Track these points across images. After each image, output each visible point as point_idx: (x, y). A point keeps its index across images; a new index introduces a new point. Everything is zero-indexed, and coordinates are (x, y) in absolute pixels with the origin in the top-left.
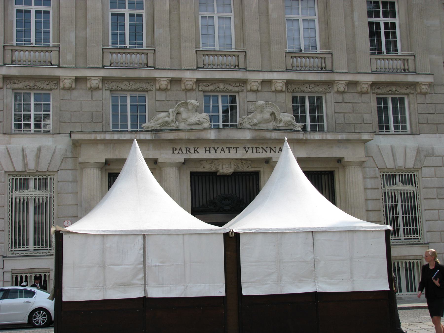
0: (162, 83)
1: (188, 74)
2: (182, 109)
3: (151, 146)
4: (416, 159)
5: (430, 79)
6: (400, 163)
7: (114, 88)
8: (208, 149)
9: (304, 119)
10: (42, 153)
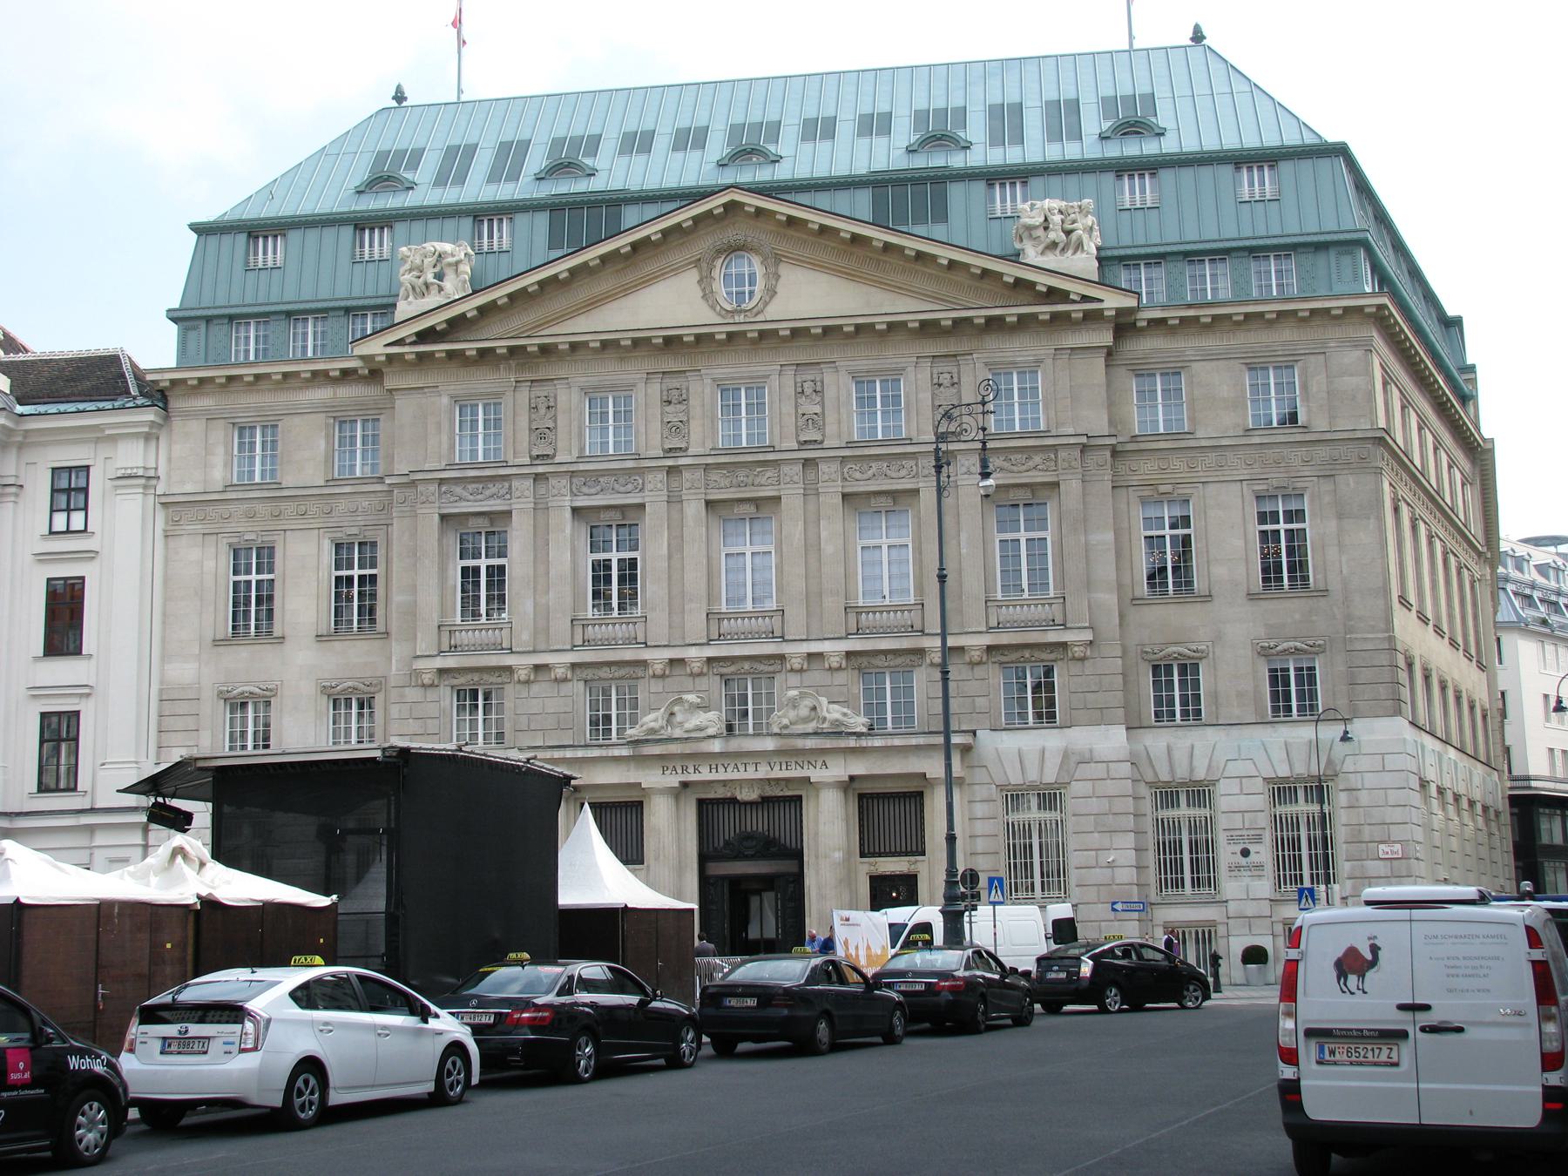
0: (656, 666)
1: (692, 653)
2: (676, 709)
3: (632, 765)
5: (1087, 636)
6: (1033, 776)
7: (589, 678)
8: (714, 766)
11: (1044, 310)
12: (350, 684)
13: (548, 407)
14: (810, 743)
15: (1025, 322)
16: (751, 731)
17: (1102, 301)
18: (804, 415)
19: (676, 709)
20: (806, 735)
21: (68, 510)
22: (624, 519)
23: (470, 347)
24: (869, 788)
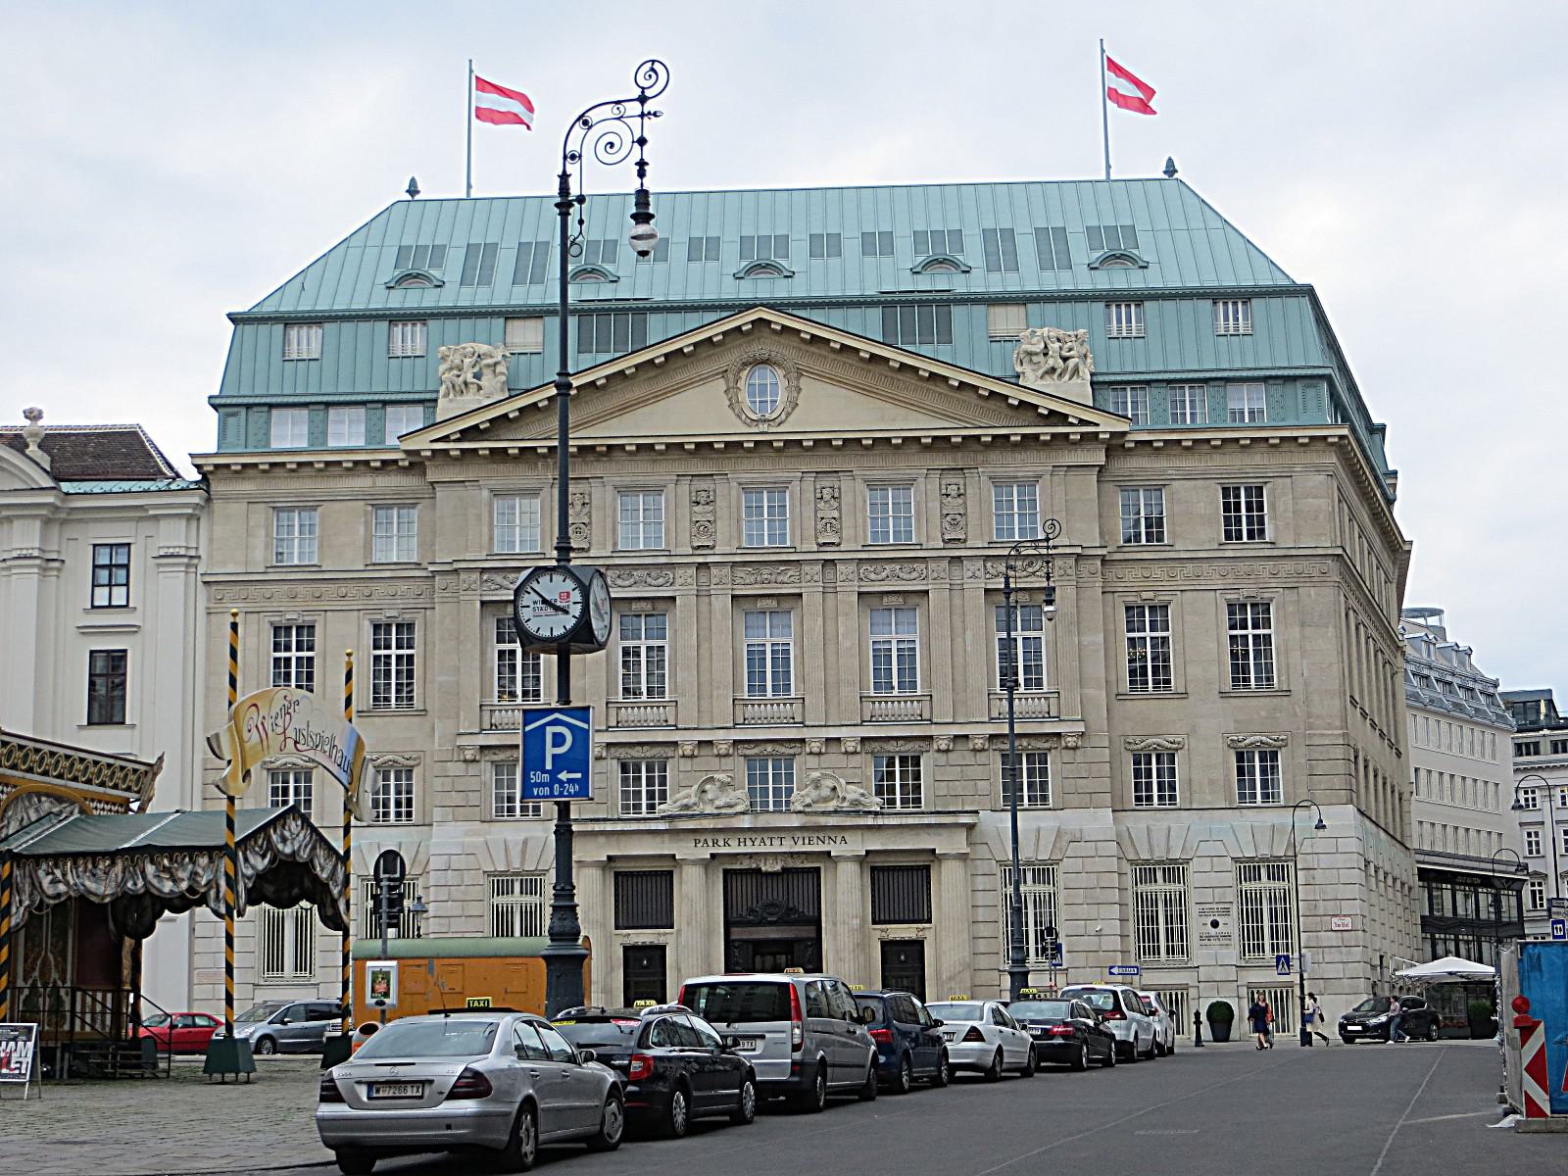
1: (720, 735)
2: (708, 787)
9: (892, 790)
11: (1045, 431)
12: (391, 757)
13: (584, 504)
14: (832, 821)
16: (771, 808)
17: (1097, 425)
19: (708, 787)
20: (829, 813)
22: (654, 609)
23: (513, 446)
24: (880, 862)
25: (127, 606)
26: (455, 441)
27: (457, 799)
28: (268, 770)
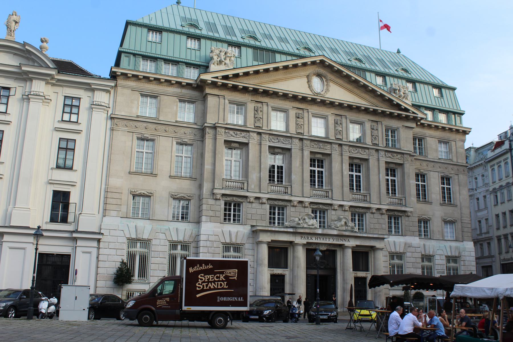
0: (295, 203)
4: (404, 248)
6: (398, 250)
8: (317, 238)
10: (238, 234)
12: (183, 195)
14: (347, 233)
15: (399, 116)
17: (418, 114)
18: (337, 130)
21: (71, 113)
23: (241, 85)
25: (77, 122)
26: (220, 79)
27: (211, 213)
28: (133, 195)
